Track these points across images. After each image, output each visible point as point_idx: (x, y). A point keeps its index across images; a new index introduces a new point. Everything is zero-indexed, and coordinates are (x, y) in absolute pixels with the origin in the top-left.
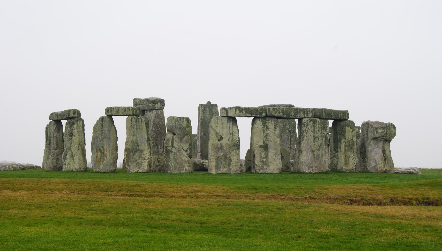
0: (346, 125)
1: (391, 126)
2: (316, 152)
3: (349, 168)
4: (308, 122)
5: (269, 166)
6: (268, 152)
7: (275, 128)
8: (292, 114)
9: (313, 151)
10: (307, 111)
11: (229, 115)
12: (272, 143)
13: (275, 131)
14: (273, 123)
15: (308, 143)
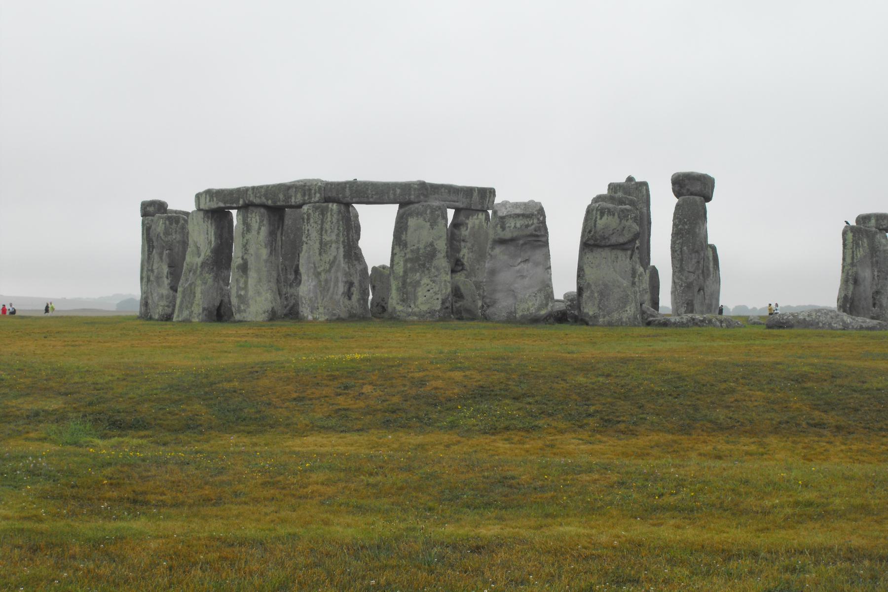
0: (411, 215)
1: (594, 212)
2: (323, 277)
3: (416, 310)
4: (310, 211)
5: (248, 306)
6: (247, 277)
7: (260, 229)
8: (281, 196)
9: (319, 274)
10: (310, 190)
11: (202, 207)
12: (252, 258)
13: (258, 233)
14: (258, 218)
15: (309, 257)
